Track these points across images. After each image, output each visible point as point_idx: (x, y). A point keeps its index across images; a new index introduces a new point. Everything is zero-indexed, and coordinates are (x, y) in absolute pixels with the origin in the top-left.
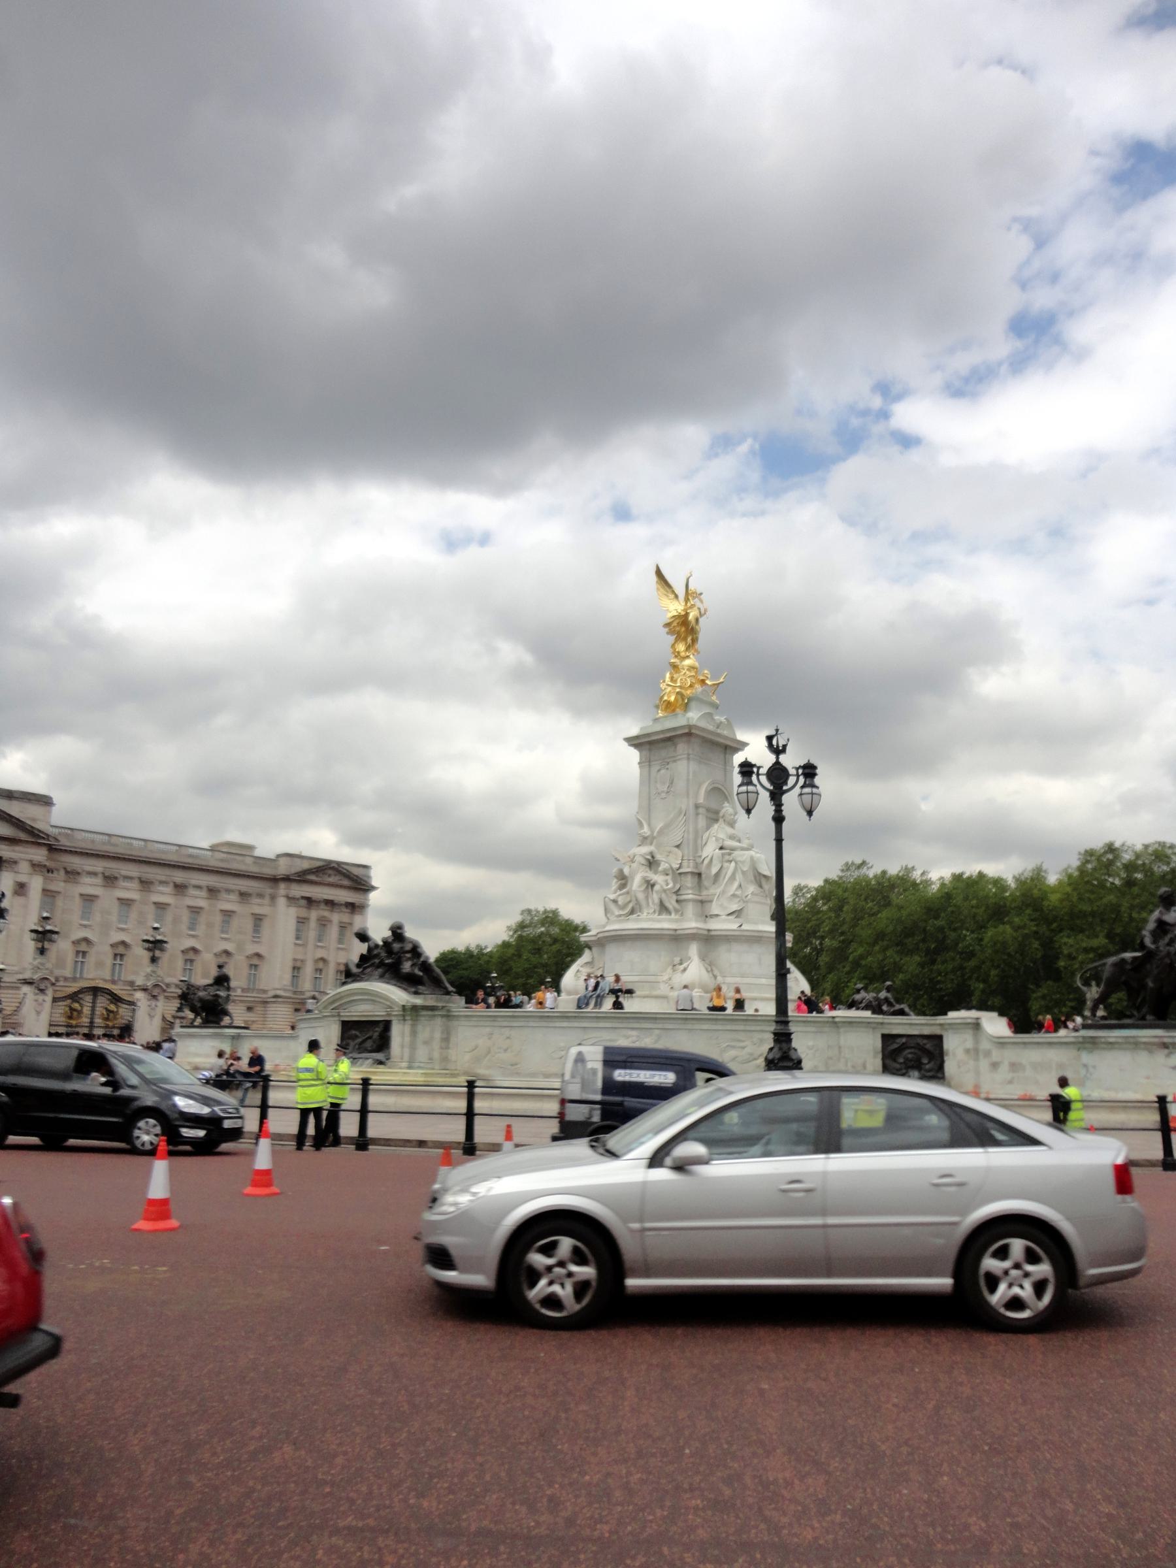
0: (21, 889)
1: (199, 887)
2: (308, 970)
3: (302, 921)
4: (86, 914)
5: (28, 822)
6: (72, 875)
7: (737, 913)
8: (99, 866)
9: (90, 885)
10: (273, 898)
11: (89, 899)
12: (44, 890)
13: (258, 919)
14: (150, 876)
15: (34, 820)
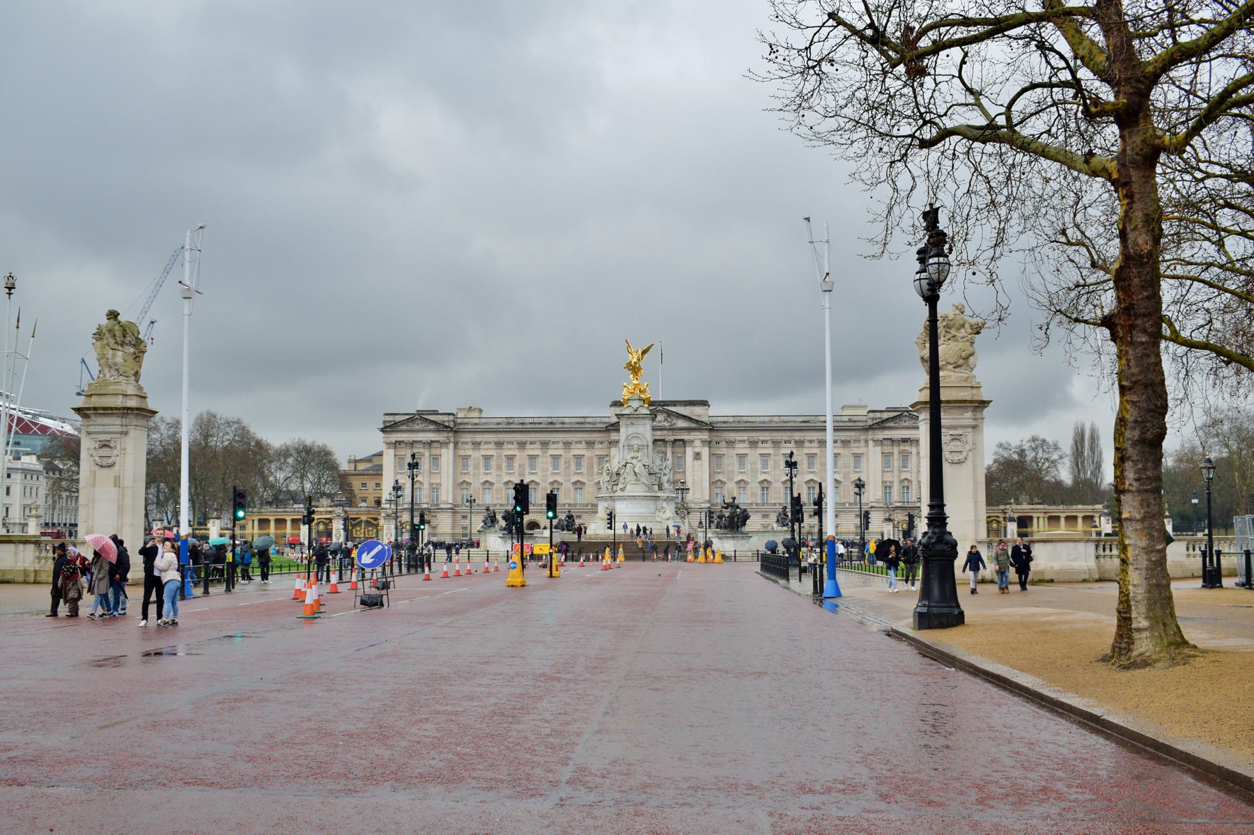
0: (697, 456)
1: (811, 442)
2: (896, 488)
3: (887, 456)
4: (742, 464)
6: (731, 444)
7: (622, 489)
8: (745, 436)
9: (741, 449)
10: (867, 441)
11: (742, 457)
13: (857, 456)
14: (779, 438)
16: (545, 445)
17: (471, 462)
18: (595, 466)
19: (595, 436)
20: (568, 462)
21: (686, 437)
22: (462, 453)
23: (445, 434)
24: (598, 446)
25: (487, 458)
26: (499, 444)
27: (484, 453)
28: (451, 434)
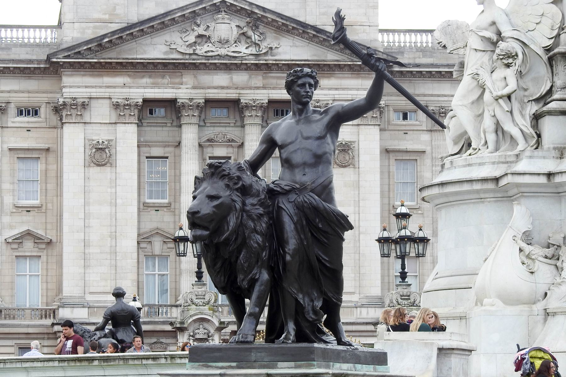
12: (387, 152)
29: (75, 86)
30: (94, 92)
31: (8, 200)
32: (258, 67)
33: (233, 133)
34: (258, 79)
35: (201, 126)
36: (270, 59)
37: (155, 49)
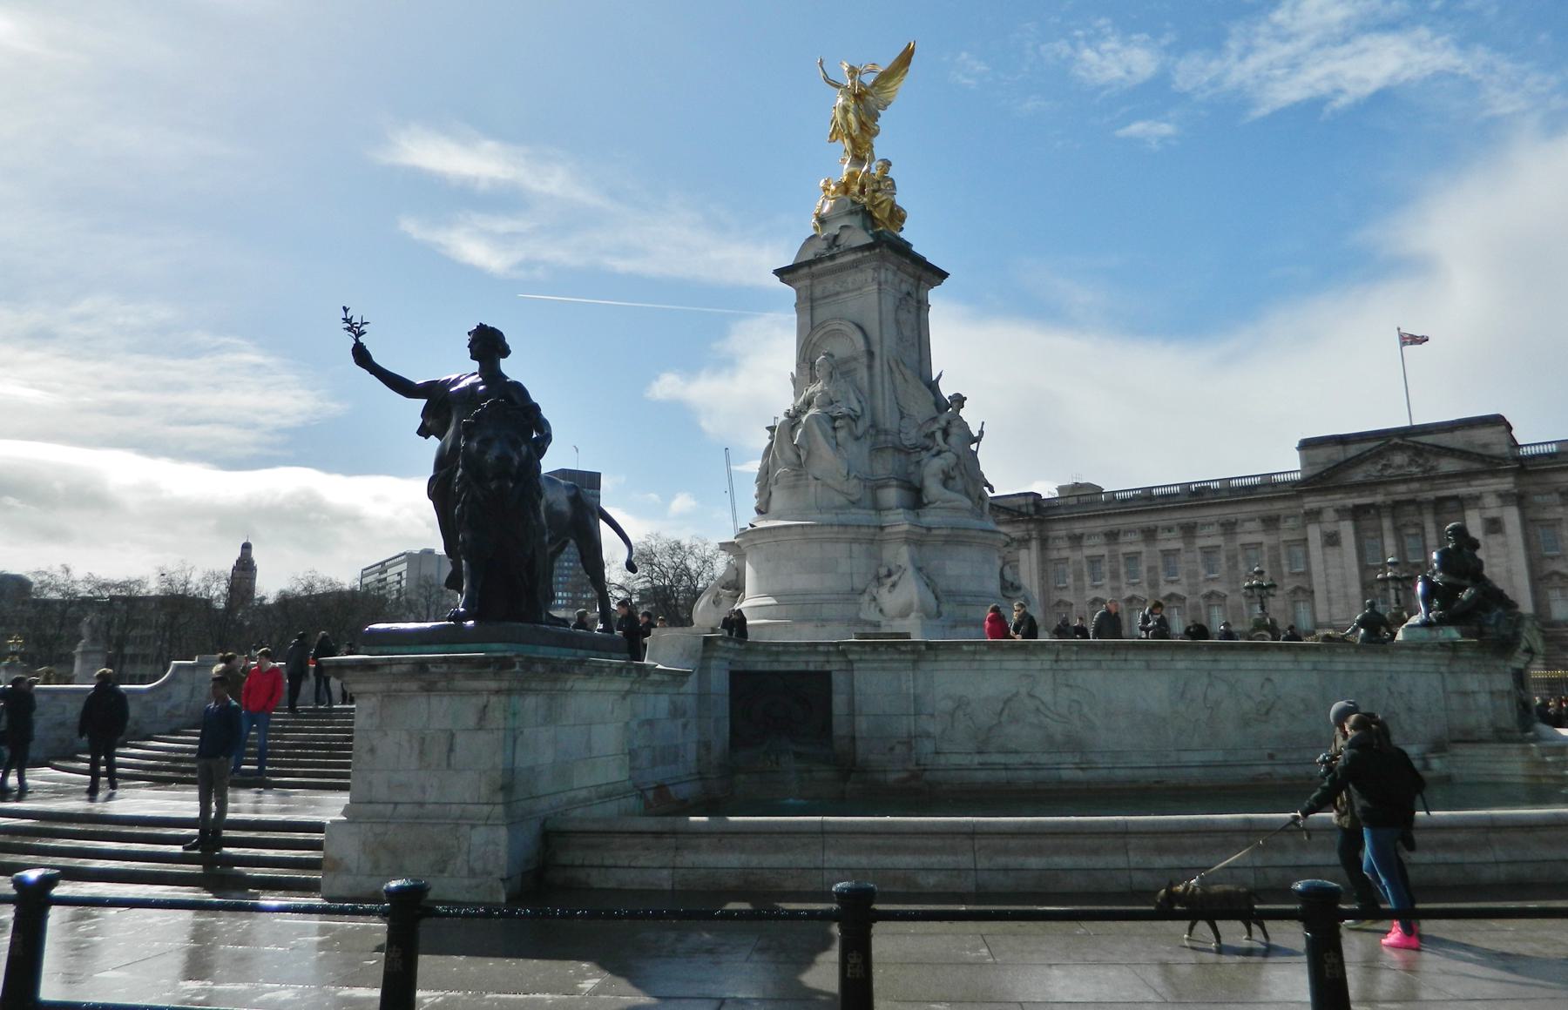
0: (1494, 526)
5: (1480, 451)
15: (1485, 446)
16: (1189, 530)
17: (1070, 570)
18: (1284, 562)
19: (1278, 507)
20: (1232, 558)
21: (1462, 490)
22: (1054, 555)
23: (1023, 527)
24: (1283, 526)
25: (1094, 561)
26: (1112, 536)
27: (1088, 552)
28: (1032, 526)
29: (1311, 502)
30: (1323, 505)
31: (1286, 569)
32: (1425, 479)
33: (1416, 519)
34: (1426, 486)
35: (1394, 518)
36: (1432, 473)
37: (1358, 475)
